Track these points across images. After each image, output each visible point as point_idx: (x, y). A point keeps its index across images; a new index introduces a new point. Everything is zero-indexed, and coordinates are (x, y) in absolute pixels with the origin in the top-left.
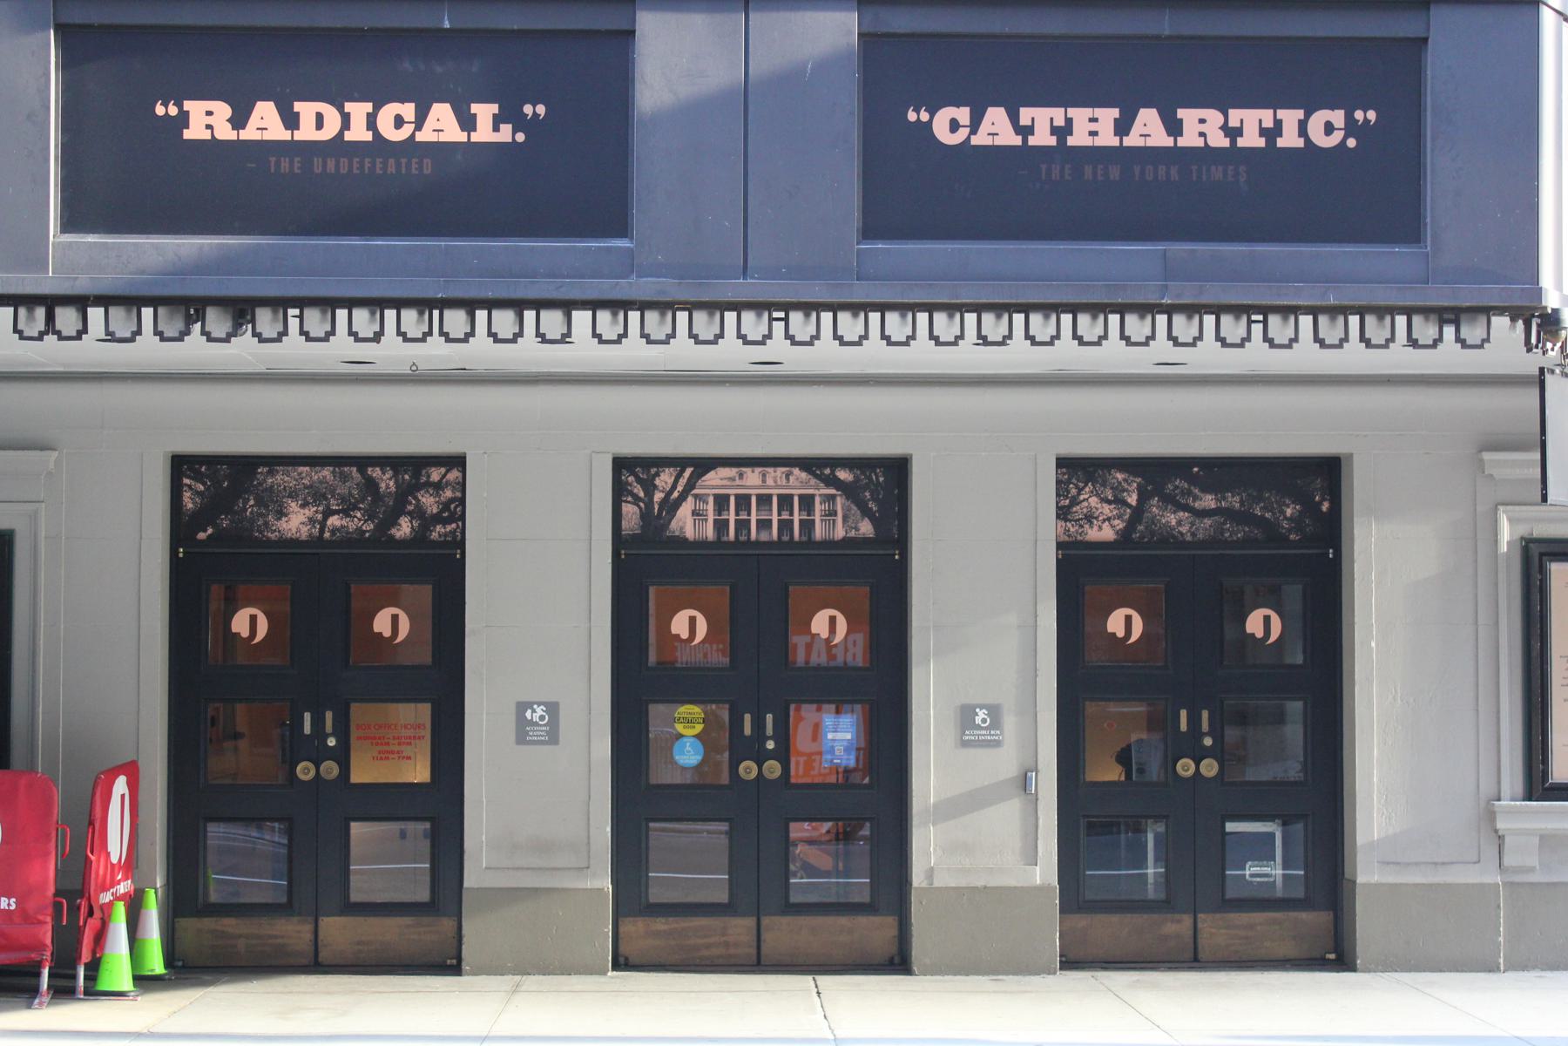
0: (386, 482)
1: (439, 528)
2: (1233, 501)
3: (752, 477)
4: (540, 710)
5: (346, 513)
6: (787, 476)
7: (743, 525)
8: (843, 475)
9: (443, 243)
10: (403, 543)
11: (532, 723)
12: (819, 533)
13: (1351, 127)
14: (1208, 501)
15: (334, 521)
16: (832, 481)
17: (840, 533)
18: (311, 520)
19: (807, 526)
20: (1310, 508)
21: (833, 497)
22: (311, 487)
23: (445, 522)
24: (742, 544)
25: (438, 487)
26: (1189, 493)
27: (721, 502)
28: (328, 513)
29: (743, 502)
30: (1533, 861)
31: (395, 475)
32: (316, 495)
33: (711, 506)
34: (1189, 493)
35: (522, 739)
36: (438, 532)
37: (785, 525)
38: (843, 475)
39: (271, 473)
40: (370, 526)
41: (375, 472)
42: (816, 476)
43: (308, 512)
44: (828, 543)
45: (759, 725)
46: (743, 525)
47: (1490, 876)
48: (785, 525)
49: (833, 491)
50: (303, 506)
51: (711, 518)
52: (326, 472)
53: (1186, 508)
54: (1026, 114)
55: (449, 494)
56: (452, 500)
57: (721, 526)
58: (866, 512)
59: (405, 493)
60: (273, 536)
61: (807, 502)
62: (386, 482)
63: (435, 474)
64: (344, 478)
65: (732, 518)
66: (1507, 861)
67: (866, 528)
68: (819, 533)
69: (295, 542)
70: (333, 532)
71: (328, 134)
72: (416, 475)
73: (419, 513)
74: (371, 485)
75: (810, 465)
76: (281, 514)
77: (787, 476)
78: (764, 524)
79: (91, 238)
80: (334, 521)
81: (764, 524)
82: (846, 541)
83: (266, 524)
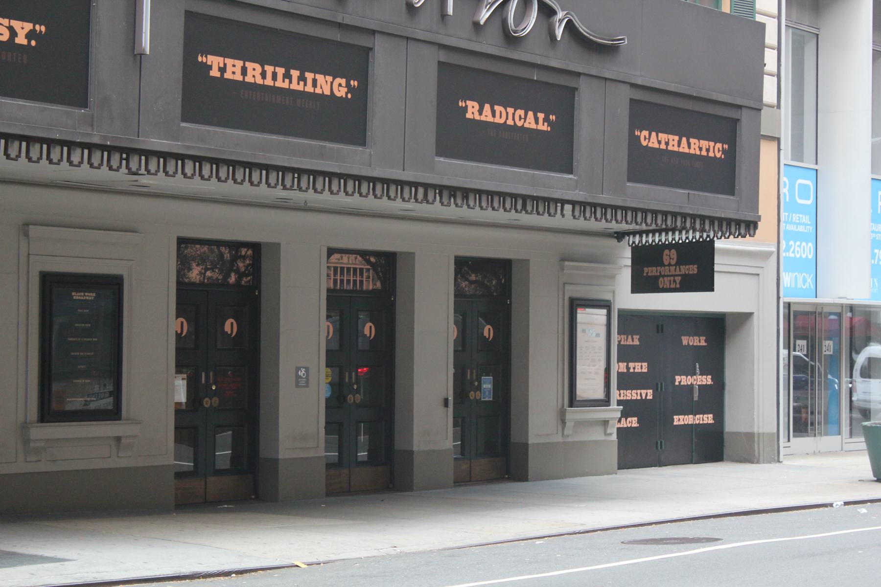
0: (227, 256)
1: (244, 279)
2: (480, 278)
3: (345, 259)
4: (303, 370)
5: (212, 269)
6: (356, 258)
7: (342, 281)
8: (373, 260)
9: (545, 173)
10: (232, 286)
11: (301, 377)
12: (365, 288)
13: (724, 151)
14: (473, 277)
15: (208, 274)
16: (369, 262)
17: (371, 287)
18: (200, 273)
19: (361, 282)
20: (499, 280)
21: (368, 270)
22: (199, 255)
23: (247, 275)
24: (342, 291)
25: (244, 258)
26: (468, 274)
27: (335, 269)
28: (206, 269)
29: (342, 269)
30: (570, 432)
31: (229, 252)
32: (202, 260)
33: (332, 272)
34: (468, 274)
35: (297, 386)
36: (245, 280)
37: (355, 281)
38: (373, 260)
39: (186, 248)
40: (220, 277)
41: (223, 249)
42: (365, 260)
43: (199, 268)
44: (368, 292)
45: (350, 378)
46: (342, 281)
47: (560, 439)
48: (355, 281)
49: (369, 267)
50: (197, 265)
51: (332, 277)
52: (206, 248)
53: (467, 280)
54: (660, 135)
55: (248, 262)
56: (249, 265)
57: (335, 281)
58: (379, 278)
59: (236, 258)
60: (186, 280)
61: (361, 270)
62: (227, 254)
63: (243, 251)
64: (212, 251)
65: (339, 278)
66: (566, 432)
67: (379, 285)
68: (365, 288)
69: (194, 284)
70: (209, 278)
71: (502, 121)
72: (237, 252)
73: (237, 271)
74: (221, 255)
75: (364, 254)
76: (190, 269)
77: (356, 258)
78: (348, 281)
79: (274, 137)
80: (208, 274)
81: (348, 281)
82: (373, 290)
83: (184, 274)
